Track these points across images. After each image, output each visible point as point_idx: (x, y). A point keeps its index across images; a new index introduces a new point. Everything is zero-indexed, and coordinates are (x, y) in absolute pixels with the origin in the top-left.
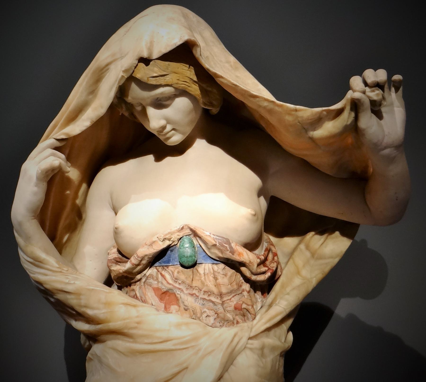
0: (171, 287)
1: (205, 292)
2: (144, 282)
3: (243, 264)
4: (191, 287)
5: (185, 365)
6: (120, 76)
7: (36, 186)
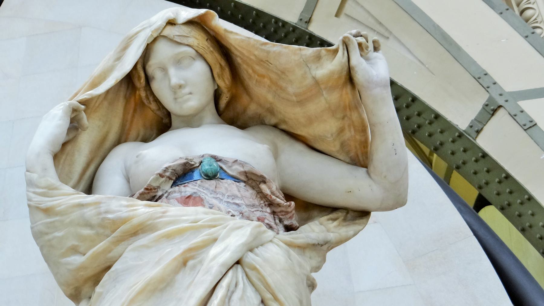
0: (195, 191)
2: (167, 197)
4: (215, 192)
5: (215, 235)
6: (150, 35)
7: (60, 120)
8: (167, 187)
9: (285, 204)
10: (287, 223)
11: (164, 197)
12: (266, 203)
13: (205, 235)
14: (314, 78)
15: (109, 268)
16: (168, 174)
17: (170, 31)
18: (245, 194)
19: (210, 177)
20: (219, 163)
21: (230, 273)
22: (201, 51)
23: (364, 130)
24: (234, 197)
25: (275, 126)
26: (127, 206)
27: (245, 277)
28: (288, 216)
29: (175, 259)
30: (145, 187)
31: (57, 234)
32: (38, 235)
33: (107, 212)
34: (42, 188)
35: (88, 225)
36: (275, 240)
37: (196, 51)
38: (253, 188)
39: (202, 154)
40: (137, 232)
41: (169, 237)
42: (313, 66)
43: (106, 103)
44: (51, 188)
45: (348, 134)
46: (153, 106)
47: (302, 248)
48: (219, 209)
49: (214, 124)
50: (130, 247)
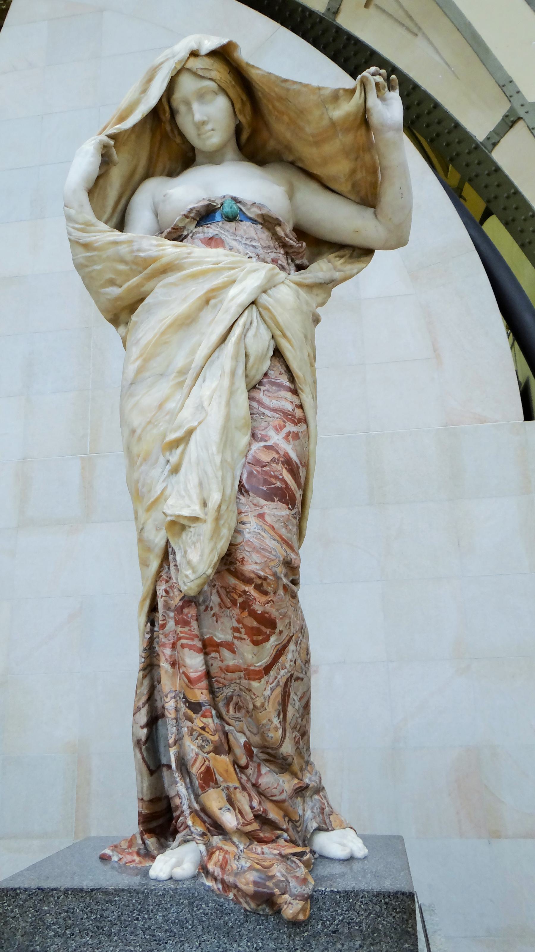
0: (217, 232)
1: (247, 238)
2: (191, 237)
3: (278, 223)
4: (235, 234)
5: (233, 278)
6: (173, 66)
8: (192, 227)
9: (298, 245)
10: (298, 262)
11: (189, 237)
12: (281, 244)
13: (226, 277)
14: (331, 119)
15: (142, 300)
16: (192, 215)
17: (194, 64)
18: (261, 235)
19: (231, 219)
20: (238, 204)
21: (246, 312)
22: (223, 85)
23: (375, 172)
24: (252, 239)
25: (292, 164)
26: (157, 246)
27: (259, 316)
28: (300, 255)
29: (199, 298)
30: (172, 226)
31: (98, 267)
32: (79, 267)
33: (139, 250)
34: (80, 224)
35: (123, 261)
36: (287, 281)
37: (219, 85)
38: (269, 230)
39: (223, 195)
40: (167, 269)
41: (194, 276)
42: (330, 107)
43: (133, 137)
44: (88, 224)
45: (359, 175)
46: (178, 140)
47: (310, 287)
48: (238, 251)
49: (236, 160)
50: (161, 284)
